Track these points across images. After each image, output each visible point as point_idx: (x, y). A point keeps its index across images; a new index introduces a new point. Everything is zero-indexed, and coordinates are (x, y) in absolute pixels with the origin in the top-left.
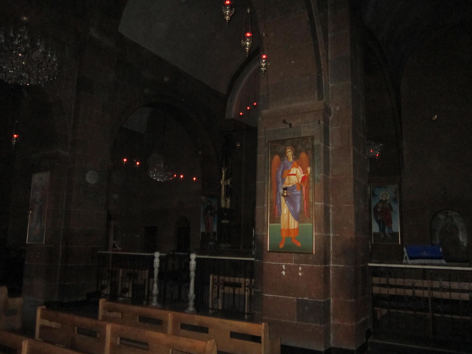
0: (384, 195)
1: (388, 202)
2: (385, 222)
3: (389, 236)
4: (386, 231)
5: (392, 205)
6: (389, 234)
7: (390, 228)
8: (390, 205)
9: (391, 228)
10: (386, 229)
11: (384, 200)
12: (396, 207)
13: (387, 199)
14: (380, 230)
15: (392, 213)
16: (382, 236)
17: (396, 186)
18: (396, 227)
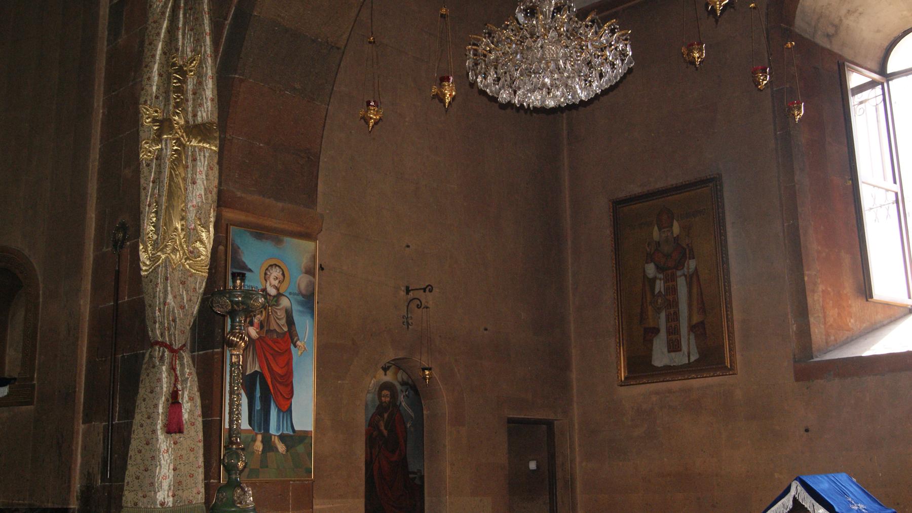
0: (275, 273)
1: (285, 302)
2: (270, 389)
3: (281, 448)
4: (273, 430)
5: (296, 317)
6: (282, 438)
7: (286, 411)
8: (290, 322)
9: (289, 411)
10: (274, 412)
11: (272, 292)
12: (306, 330)
13: (281, 291)
14: (250, 424)
15: (292, 347)
16: (259, 446)
17: (309, 246)
18: (304, 413)
